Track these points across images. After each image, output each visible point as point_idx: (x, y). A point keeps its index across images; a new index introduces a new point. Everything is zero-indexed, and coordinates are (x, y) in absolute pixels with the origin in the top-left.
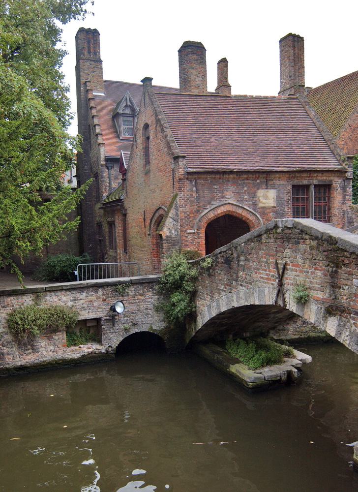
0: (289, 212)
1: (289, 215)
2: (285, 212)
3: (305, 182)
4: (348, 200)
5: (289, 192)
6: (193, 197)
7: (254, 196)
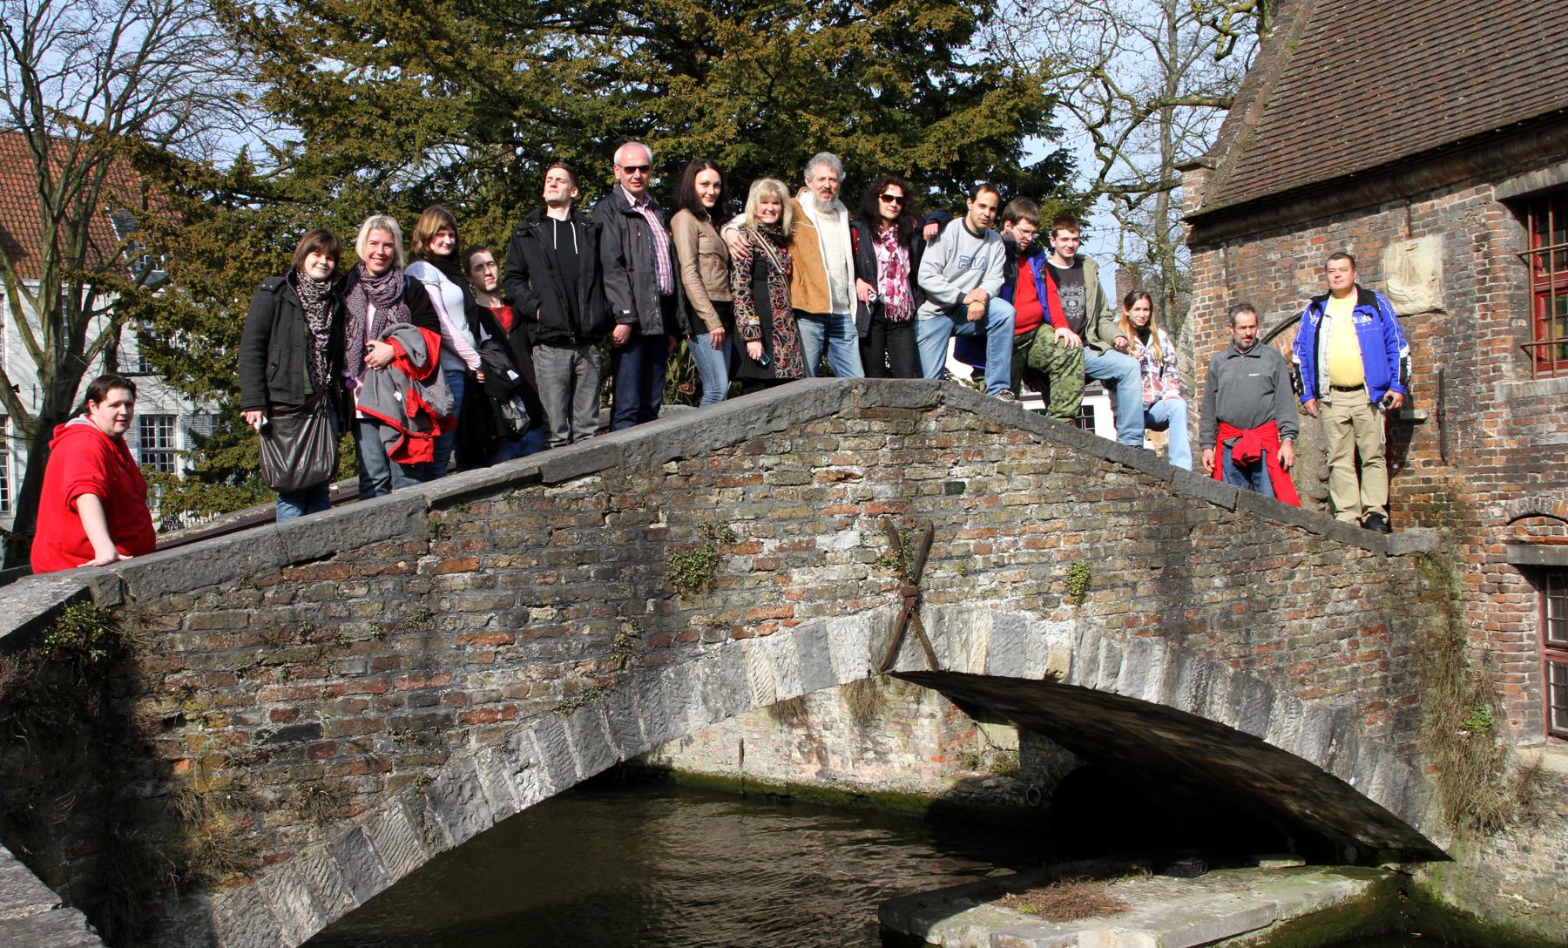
0: (1487, 326)
1: (1489, 343)
2: (1472, 327)
6: (1221, 305)
7: (1376, 273)
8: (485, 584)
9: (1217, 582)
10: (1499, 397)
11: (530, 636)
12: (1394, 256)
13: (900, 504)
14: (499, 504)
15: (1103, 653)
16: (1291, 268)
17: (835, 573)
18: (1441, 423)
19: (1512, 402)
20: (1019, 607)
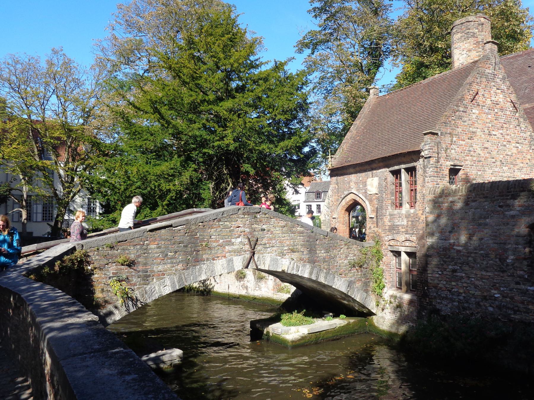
3: (396, 168)
4: (428, 182)
5: (386, 179)
8: (159, 247)
9: (322, 252)
10: (388, 214)
11: (168, 259)
12: (369, 181)
13: (251, 233)
14: (163, 231)
15: (295, 266)
16: (349, 182)
17: (235, 247)
18: (377, 218)
19: (391, 215)
20: (276, 256)
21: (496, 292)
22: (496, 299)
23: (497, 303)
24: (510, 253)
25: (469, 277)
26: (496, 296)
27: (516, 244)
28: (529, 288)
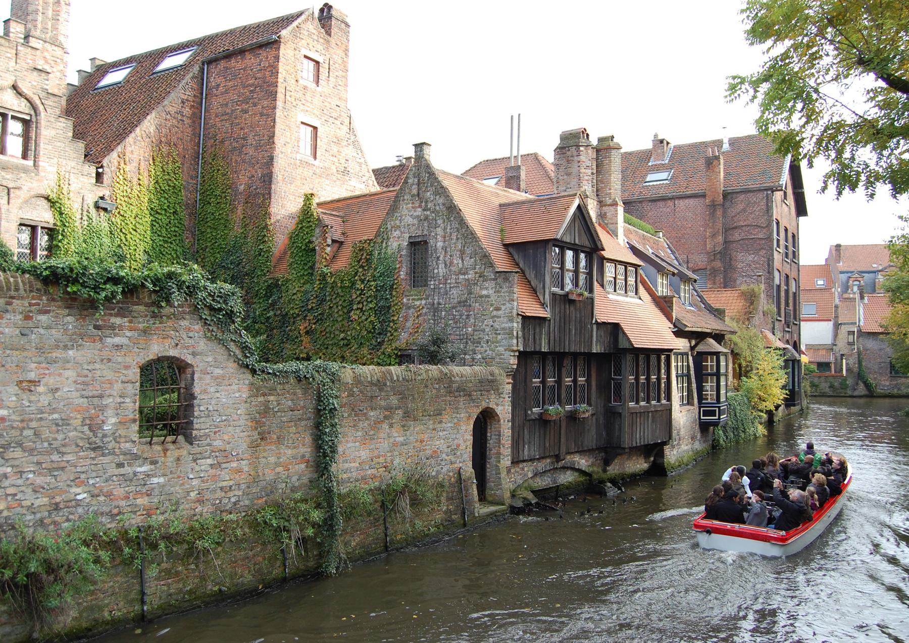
21: (79, 490)
22: (78, 503)
23: (80, 510)
24: (110, 412)
25: (21, 473)
26: (79, 497)
27: (120, 396)
28: (139, 469)
